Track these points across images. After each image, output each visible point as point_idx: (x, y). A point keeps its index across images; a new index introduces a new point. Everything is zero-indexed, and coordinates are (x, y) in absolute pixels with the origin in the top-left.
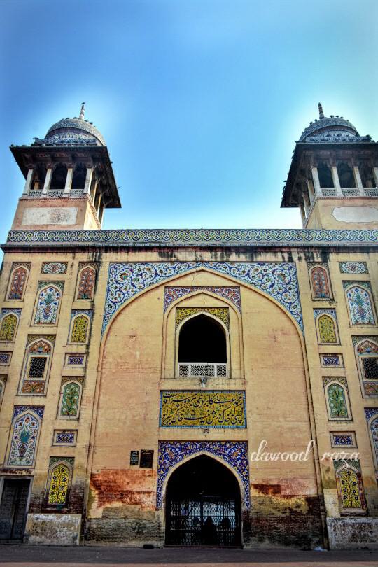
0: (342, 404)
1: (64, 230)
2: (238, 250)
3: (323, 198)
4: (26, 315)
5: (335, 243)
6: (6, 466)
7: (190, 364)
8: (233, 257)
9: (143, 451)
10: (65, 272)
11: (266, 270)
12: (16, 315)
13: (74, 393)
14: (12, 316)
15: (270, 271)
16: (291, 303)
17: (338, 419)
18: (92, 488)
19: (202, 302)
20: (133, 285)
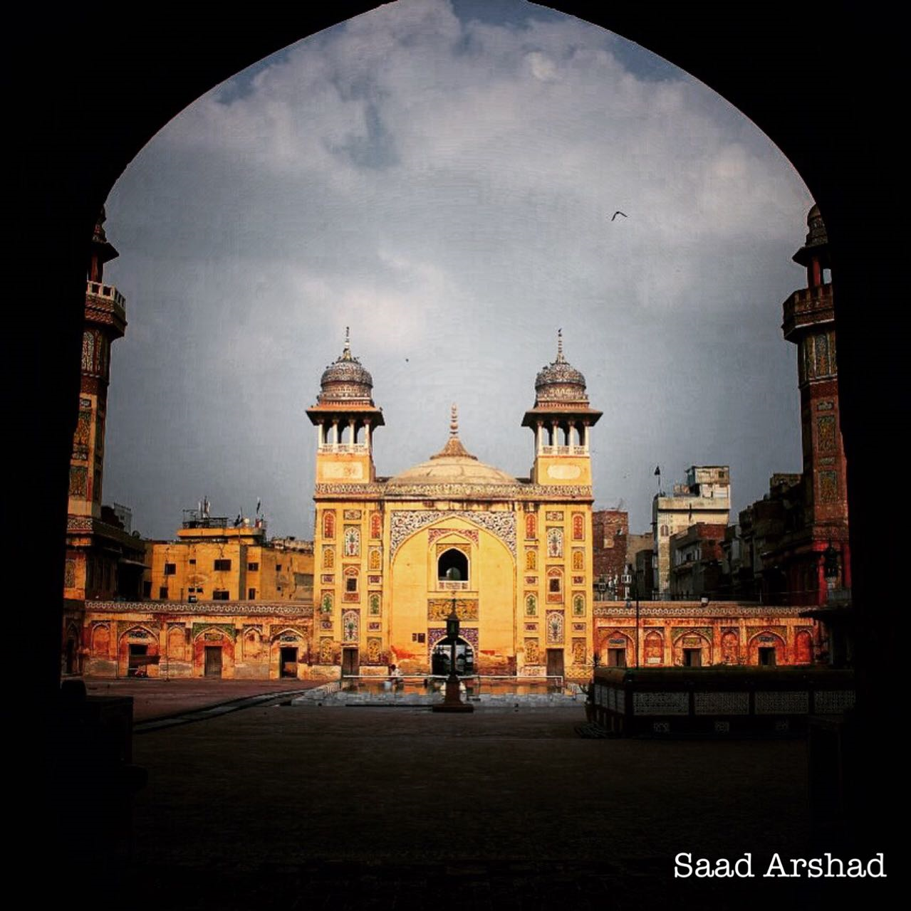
0: (534, 607)
1: (353, 482)
2: (478, 502)
3: (543, 457)
4: (339, 550)
5: (546, 498)
6: (343, 642)
7: (445, 582)
8: (475, 507)
9: (419, 634)
10: (360, 518)
11: (496, 518)
12: (331, 549)
13: (377, 600)
14: (329, 550)
15: (499, 518)
16: (510, 543)
17: (530, 616)
18: (392, 653)
19: (453, 541)
20: (407, 528)
